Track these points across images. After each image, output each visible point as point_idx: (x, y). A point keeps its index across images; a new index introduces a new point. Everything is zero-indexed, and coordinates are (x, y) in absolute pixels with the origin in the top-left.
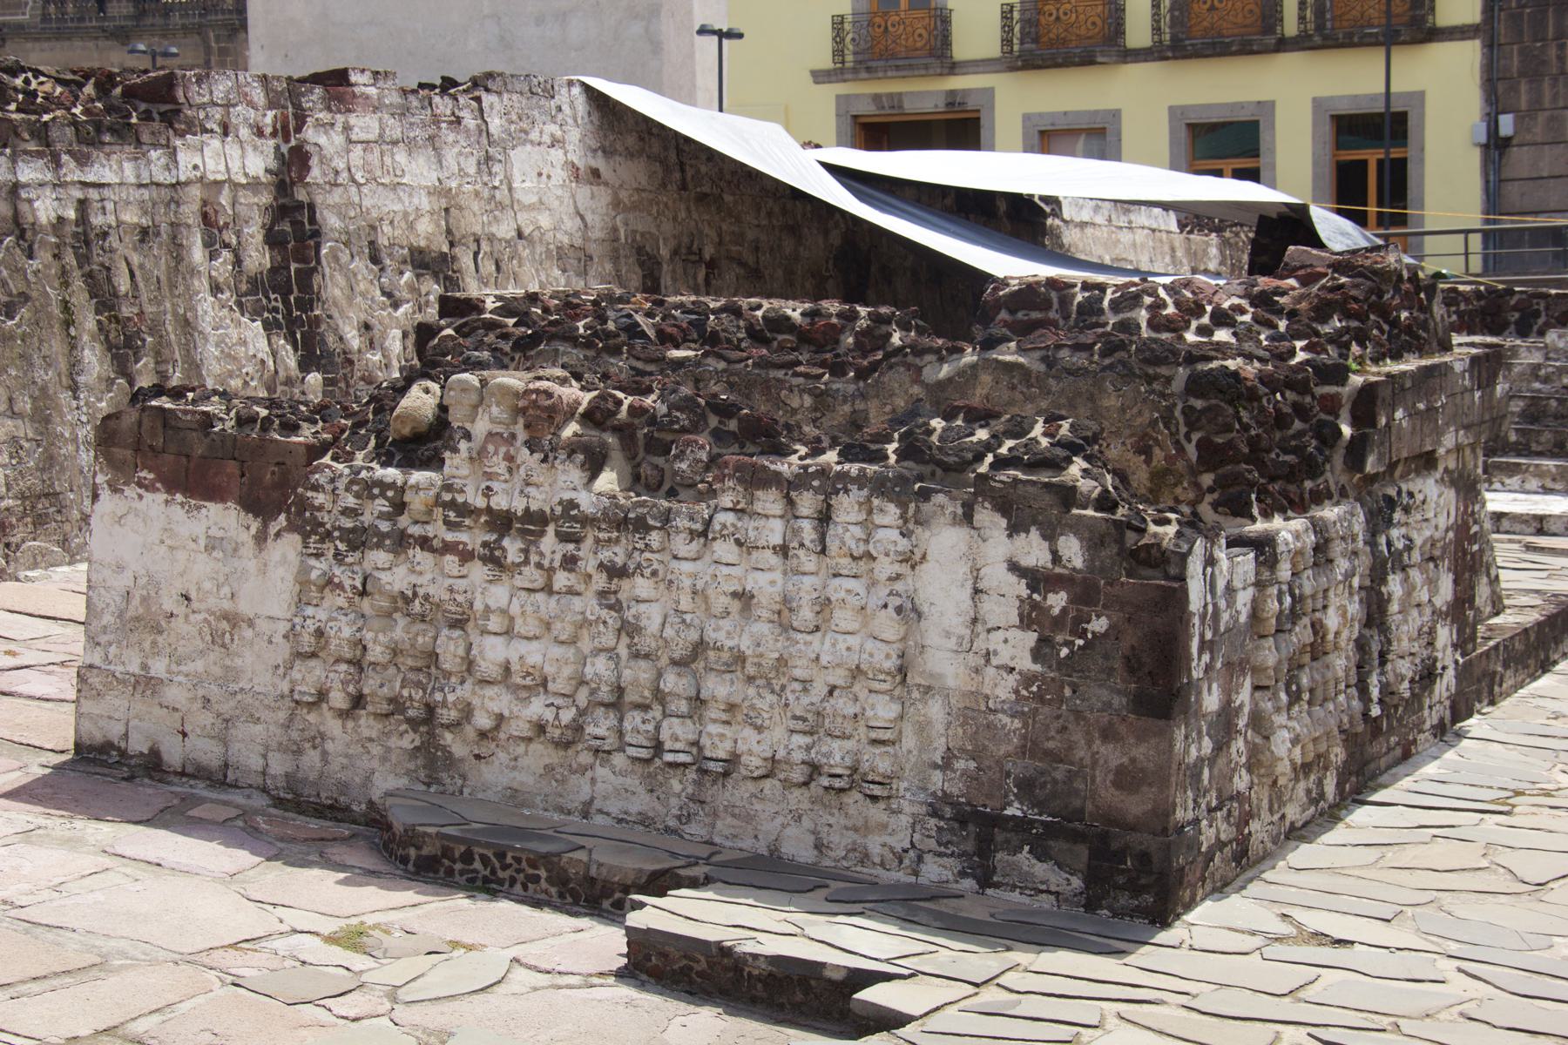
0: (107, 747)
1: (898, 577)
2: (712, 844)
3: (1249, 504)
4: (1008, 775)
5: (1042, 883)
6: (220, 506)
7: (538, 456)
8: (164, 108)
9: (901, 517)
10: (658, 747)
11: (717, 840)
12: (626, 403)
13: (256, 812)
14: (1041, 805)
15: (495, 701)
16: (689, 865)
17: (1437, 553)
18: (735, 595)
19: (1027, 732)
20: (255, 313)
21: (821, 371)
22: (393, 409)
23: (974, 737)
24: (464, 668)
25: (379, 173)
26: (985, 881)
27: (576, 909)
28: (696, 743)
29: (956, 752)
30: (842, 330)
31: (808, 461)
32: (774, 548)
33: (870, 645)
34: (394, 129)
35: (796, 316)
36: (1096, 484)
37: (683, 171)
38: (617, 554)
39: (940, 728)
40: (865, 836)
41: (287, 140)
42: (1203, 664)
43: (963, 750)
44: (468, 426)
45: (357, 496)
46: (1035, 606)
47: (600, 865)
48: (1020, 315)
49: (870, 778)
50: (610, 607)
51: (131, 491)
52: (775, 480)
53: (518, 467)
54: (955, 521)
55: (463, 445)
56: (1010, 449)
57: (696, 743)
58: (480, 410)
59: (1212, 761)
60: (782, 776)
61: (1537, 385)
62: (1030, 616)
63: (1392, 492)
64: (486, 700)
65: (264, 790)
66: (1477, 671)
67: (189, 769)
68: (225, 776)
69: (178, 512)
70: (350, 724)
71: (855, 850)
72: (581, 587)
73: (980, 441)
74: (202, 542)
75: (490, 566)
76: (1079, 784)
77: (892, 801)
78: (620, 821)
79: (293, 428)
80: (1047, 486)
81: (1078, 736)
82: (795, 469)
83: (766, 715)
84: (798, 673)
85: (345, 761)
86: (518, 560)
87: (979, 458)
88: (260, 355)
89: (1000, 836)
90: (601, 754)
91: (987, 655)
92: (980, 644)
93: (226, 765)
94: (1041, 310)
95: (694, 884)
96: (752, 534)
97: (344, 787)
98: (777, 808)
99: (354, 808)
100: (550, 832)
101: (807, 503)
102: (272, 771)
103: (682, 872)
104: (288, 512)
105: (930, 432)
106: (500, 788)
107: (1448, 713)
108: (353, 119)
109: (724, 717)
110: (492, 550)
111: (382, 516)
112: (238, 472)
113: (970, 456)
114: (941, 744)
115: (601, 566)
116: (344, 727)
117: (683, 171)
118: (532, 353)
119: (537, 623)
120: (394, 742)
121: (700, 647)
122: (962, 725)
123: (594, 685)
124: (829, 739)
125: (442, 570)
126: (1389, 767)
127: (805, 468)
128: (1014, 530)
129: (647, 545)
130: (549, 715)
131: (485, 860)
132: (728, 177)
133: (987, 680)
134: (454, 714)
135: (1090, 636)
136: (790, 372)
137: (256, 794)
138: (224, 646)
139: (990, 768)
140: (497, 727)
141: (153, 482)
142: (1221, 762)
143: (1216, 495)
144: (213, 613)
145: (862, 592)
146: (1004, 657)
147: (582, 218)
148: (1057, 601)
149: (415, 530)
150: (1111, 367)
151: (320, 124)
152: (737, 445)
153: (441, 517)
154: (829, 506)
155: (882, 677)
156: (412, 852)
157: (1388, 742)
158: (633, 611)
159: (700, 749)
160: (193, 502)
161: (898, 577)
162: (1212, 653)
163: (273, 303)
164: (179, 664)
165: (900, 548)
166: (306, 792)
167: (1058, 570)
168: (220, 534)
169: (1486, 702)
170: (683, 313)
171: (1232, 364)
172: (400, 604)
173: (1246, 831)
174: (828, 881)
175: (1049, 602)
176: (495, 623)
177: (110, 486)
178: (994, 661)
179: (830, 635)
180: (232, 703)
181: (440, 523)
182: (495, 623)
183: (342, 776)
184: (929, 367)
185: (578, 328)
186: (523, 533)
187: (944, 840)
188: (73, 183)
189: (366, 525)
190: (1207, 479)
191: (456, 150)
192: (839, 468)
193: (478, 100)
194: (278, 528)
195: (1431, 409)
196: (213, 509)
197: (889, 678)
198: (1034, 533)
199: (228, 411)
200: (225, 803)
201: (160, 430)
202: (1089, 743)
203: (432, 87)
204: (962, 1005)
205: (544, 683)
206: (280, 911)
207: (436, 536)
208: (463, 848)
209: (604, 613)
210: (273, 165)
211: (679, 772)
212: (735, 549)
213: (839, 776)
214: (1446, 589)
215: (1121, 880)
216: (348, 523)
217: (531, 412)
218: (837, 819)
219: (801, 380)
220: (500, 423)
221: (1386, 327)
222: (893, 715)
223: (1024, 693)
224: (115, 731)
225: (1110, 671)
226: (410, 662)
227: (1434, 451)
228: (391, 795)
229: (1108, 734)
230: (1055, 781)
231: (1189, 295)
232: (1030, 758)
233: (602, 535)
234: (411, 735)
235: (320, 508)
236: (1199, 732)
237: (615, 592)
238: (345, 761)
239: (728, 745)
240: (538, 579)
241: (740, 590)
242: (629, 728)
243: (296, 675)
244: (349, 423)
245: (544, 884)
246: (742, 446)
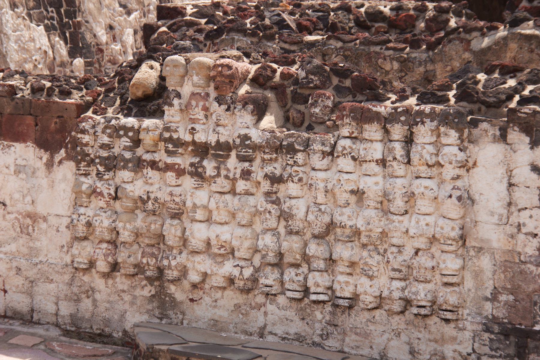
1: (458, 177)
2: (343, 352)
6: (23, 145)
7: (224, 107)
9: (459, 138)
10: (306, 291)
11: (346, 349)
12: (279, 71)
13: (53, 339)
18: (352, 192)
20: (40, 21)
21: (404, 45)
22: (130, 80)
24: (181, 243)
28: (330, 288)
29: (500, 290)
30: (417, 18)
32: (377, 161)
33: (441, 222)
35: (387, 10)
38: (276, 169)
39: (489, 274)
40: (442, 345)
43: (504, 288)
44: (179, 89)
45: (110, 136)
49: (444, 308)
50: (273, 202)
52: (376, 117)
53: (212, 114)
54: (495, 140)
55: (176, 102)
56: (531, 92)
57: (330, 288)
58: (186, 78)
60: (387, 308)
64: (196, 264)
65: (57, 325)
67: (9, 314)
68: (32, 317)
70: (110, 282)
71: (436, 354)
72: (254, 190)
73: (510, 87)
74: (12, 169)
75: (196, 178)
77: (459, 322)
78: (284, 339)
79: (67, 94)
82: (389, 110)
83: (375, 269)
84: (395, 241)
85: (108, 305)
86: (213, 174)
87: (510, 98)
88: (44, 48)
89: (531, 344)
90: (270, 297)
91: (519, 227)
92: (514, 219)
93: (32, 310)
96: (362, 153)
97: (107, 322)
98: (384, 328)
99: (115, 335)
100: (239, 347)
104: (66, 148)
105: (477, 82)
106: (206, 320)
109: (348, 270)
110: (196, 168)
111: (126, 148)
112: (33, 123)
113: (504, 97)
114: (490, 285)
115: (266, 176)
116: (106, 283)
118: (218, 41)
119: (227, 214)
120: (138, 292)
121: (331, 226)
122: (503, 272)
123: (264, 253)
124: (416, 283)
125: (165, 181)
127: (396, 109)
129: (295, 162)
130: (236, 272)
133: (519, 242)
134: (176, 274)
136: (384, 47)
137: (52, 328)
138: (28, 234)
139: (523, 299)
140: (203, 281)
144: (21, 214)
145: (435, 188)
149: (147, 157)
152: (351, 96)
153: (163, 149)
154: (412, 133)
155: (450, 242)
158: (287, 204)
159: (333, 292)
160: (6, 143)
161: (458, 177)
163: (51, 14)
165: (459, 159)
166: (84, 325)
168: (24, 163)
170: (313, 11)
172: (139, 204)
176: (200, 215)
178: (524, 230)
179: (415, 216)
180: (35, 271)
181: (163, 151)
182: (200, 215)
183: (106, 315)
184: (475, 40)
185: (246, 24)
186: (216, 156)
187: (495, 347)
189: (116, 155)
192: (417, 108)
194: (60, 158)
196: (18, 147)
197: (454, 243)
199: (26, 84)
200: (33, 335)
205: (232, 252)
207: (160, 160)
209: (269, 206)
211: (320, 306)
212: (352, 162)
213: (424, 307)
216: (104, 154)
217: (218, 79)
219: (391, 52)
220: (199, 86)
222: (457, 267)
226: (147, 241)
228: (138, 326)
234: (149, 288)
235: (87, 145)
237: (276, 193)
238: (108, 305)
239: (351, 289)
240: (227, 186)
241: (356, 189)
242: (288, 279)
243: (75, 251)
244: (103, 89)
246: (354, 96)
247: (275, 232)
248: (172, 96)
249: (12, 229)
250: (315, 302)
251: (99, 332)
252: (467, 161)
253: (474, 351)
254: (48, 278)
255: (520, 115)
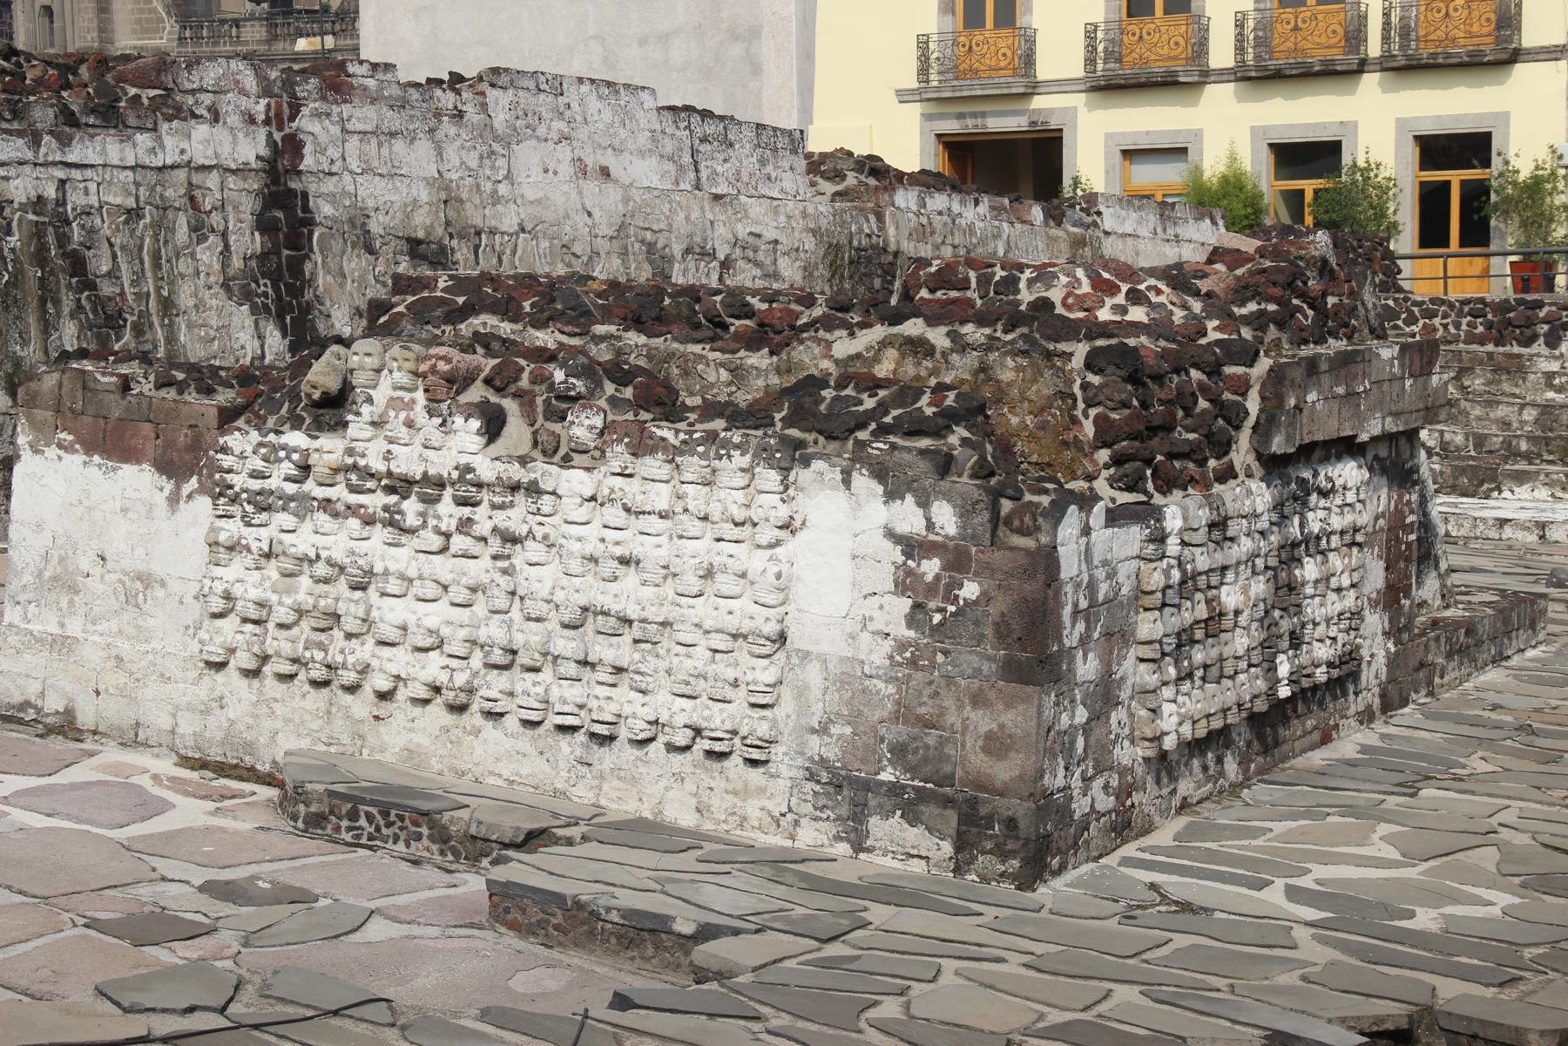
0: (26, 705)
1: (778, 543)
3: (1143, 478)
4: (882, 740)
5: (913, 847)
6: (136, 468)
8: (153, 93)
11: (603, 802)
12: (528, 370)
14: (913, 770)
15: (399, 660)
16: (568, 825)
17: (1359, 538)
19: (900, 698)
20: (247, 296)
23: (849, 703)
25: (375, 163)
26: (859, 848)
27: (454, 867)
28: (581, 707)
29: (832, 717)
31: (698, 426)
34: (393, 120)
36: (969, 452)
37: (697, 171)
39: (816, 692)
40: (745, 800)
41: (280, 129)
42: (1076, 634)
45: (266, 460)
46: (909, 573)
47: (480, 823)
48: (939, 294)
49: (748, 742)
50: (505, 572)
51: (52, 452)
55: (365, 409)
59: (1087, 729)
61: (1551, 395)
62: (906, 582)
63: (1307, 474)
64: (384, 662)
66: (1413, 662)
68: (137, 735)
69: (93, 471)
71: (735, 813)
75: (390, 529)
76: (950, 750)
77: (770, 765)
80: (923, 452)
81: (949, 702)
82: (682, 436)
84: (682, 637)
85: (251, 721)
87: (862, 426)
93: (138, 724)
94: (958, 290)
95: (570, 842)
99: (258, 767)
100: (440, 792)
101: (693, 466)
102: (180, 730)
103: (560, 832)
104: (200, 474)
106: (397, 750)
107: (1377, 701)
108: (346, 109)
109: (610, 679)
112: (153, 435)
115: (495, 530)
116: (250, 686)
117: (697, 171)
126: (1304, 751)
128: (891, 495)
130: (443, 678)
131: (370, 818)
132: (746, 179)
135: (961, 602)
136: (708, 347)
138: (137, 606)
139: (865, 733)
141: (72, 444)
142: (1098, 732)
143: (1112, 471)
144: (127, 574)
146: (878, 625)
147: (590, 214)
148: (931, 567)
149: (321, 493)
150: (1012, 342)
151: (317, 115)
156: (302, 808)
157: (1303, 725)
160: (110, 464)
162: (1087, 621)
164: (94, 624)
167: (932, 537)
168: (136, 495)
169: (1423, 692)
171: (1132, 342)
173: (1129, 803)
174: (703, 843)
175: (922, 569)
177: (31, 446)
178: (870, 628)
183: (248, 736)
184: (839, 342)
185: (522, 308)
187: (820, 804)
188: (54, 164)
190: (1103, 455)
191: (458, 143)
192: (723, 434)
193: (483, 94)
194: (189, 490)
195: (1351, 394)
196: (128, 470)
198: (909, 499)
201: (79, 394)
202: (961, 707)
203: (440, 82)
204: (802, 958)
205: (440, 647)
206: (155, 862)
207: (339, 500)
208: (349, 806)
210: (264, 151)
212: (624, 514)
213: (721, 739)
214: (1376, 577)
215: (989, 845)
216: (256, 485)
217: (431, 377)
218: (719, 783)
219: (718, 355)
221: (1310, 313)
223: (898, 658)
224: (32, 690)
225: (980, 638)
227: (1355, 436)
229: (978, 700)
230: (927, 747)
231: (1106, 275)
232: (903, 724)
233: (495, 499)
236: (1072, 701)
237: (509, 557)
238: (251, 721)
240: (436, 542)
241: (628, 556)
242: (520, 691)
245: (425, 842)
247: (506, 617)
248: (359, 400)
249: (113, 598)
250: (563, 729)
251: (235, 761)
252: (791, 517)
253: (790, 810)
254: (162, 675)
255: (870, 450)
